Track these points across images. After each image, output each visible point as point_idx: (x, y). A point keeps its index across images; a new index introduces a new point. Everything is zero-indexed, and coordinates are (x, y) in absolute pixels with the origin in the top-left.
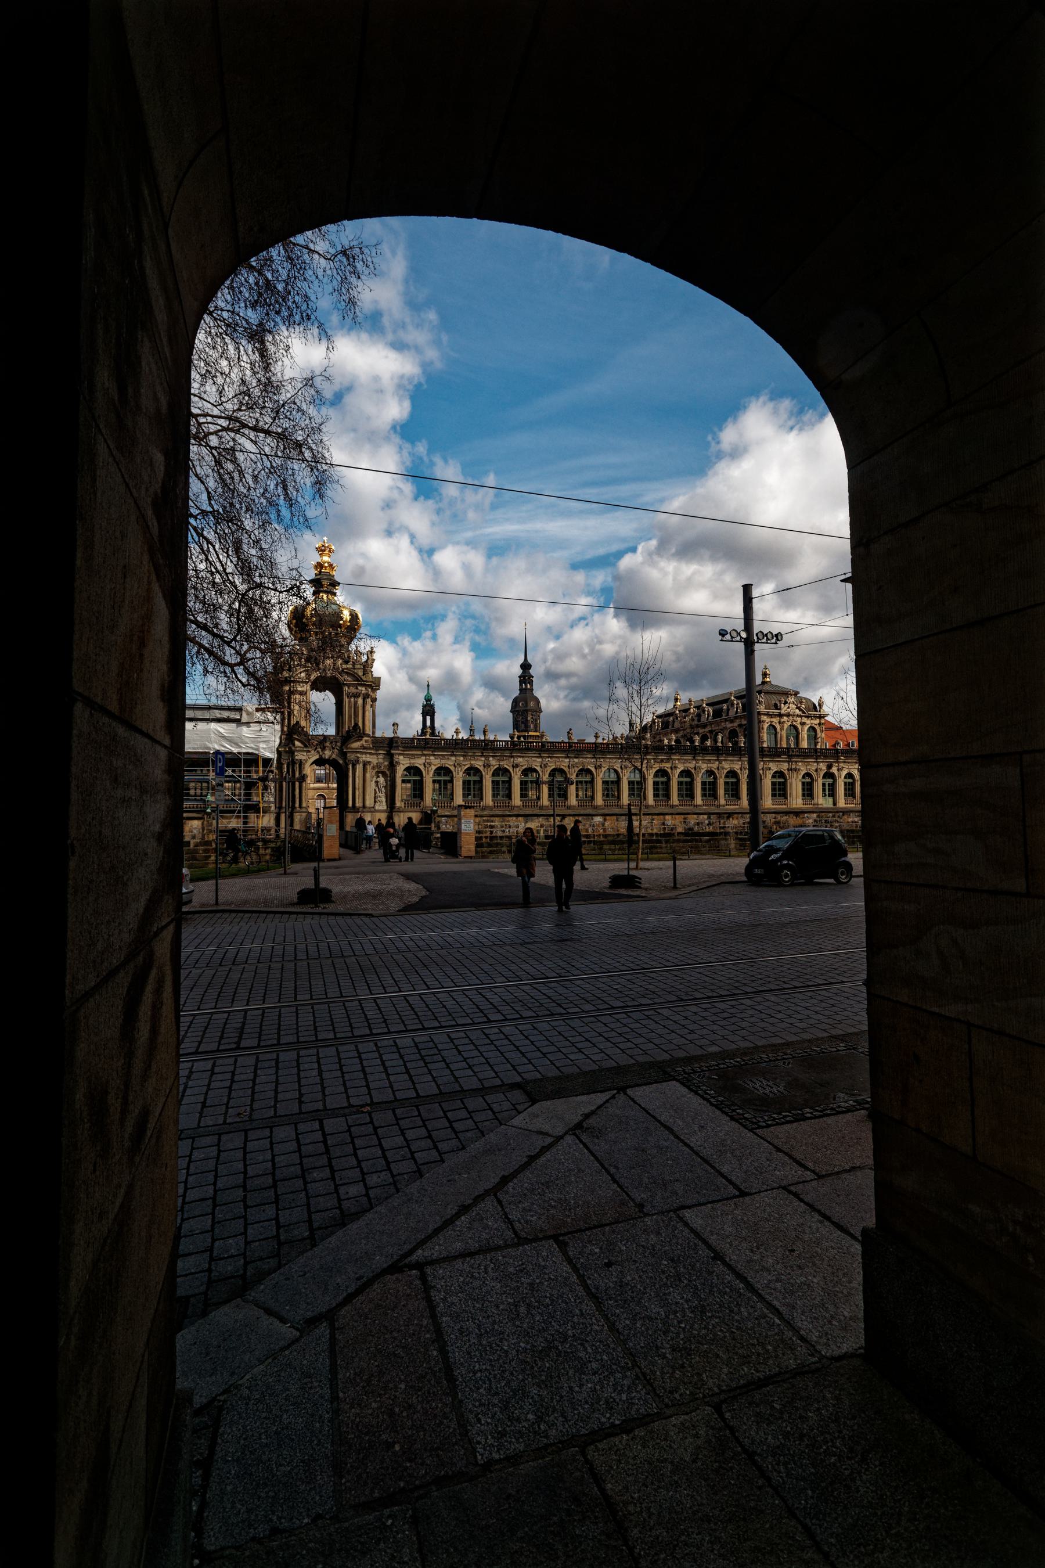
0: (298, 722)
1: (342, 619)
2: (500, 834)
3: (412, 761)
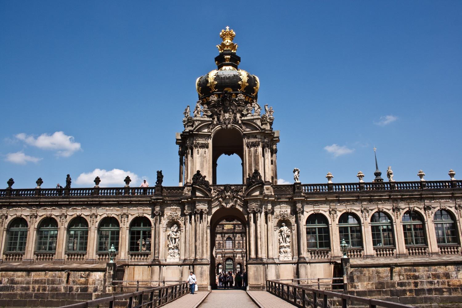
0: (198, 172)
1: (240, 80)
2: (426, 287)
3: (316, 208)
